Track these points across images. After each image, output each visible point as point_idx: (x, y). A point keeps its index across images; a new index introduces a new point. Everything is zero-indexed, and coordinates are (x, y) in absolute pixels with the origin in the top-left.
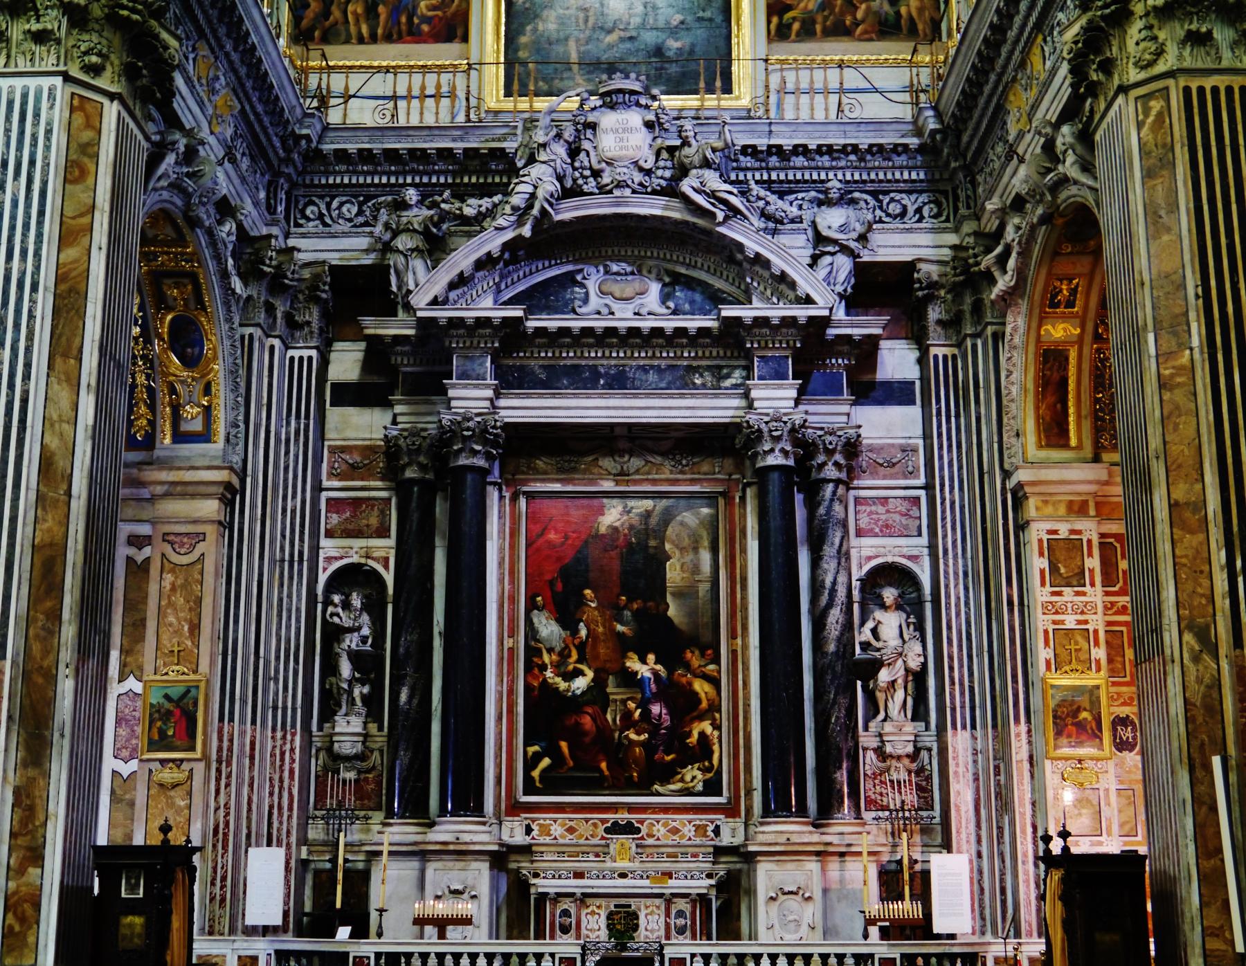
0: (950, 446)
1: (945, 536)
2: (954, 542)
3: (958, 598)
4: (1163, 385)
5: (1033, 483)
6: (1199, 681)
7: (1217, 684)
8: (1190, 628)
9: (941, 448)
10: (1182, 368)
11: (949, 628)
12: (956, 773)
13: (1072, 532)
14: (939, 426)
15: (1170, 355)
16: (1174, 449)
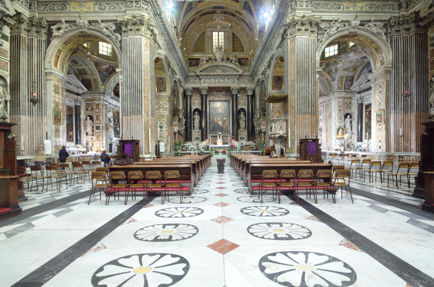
0: (24, 56)
1: (22, 75)
2: (24, 77)
3: (24, 88)
4: (144, 80)
5: (54, 73)
6: (146, 119)
7: (149, 120)
8: (146, 112)
9: (22, 56)
10: (147, 79)
11: (22, 94)
12: (22, 124)
13: (58, 84)
14: (22, 51)
15: (146, 76)
16: (145, 89)
